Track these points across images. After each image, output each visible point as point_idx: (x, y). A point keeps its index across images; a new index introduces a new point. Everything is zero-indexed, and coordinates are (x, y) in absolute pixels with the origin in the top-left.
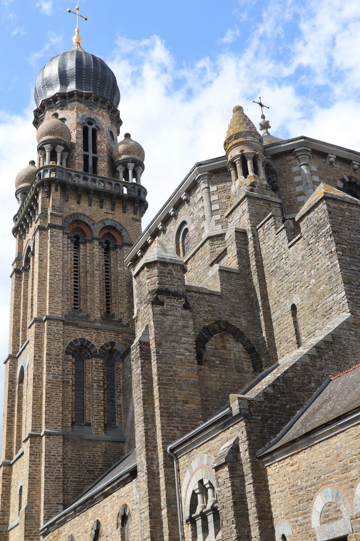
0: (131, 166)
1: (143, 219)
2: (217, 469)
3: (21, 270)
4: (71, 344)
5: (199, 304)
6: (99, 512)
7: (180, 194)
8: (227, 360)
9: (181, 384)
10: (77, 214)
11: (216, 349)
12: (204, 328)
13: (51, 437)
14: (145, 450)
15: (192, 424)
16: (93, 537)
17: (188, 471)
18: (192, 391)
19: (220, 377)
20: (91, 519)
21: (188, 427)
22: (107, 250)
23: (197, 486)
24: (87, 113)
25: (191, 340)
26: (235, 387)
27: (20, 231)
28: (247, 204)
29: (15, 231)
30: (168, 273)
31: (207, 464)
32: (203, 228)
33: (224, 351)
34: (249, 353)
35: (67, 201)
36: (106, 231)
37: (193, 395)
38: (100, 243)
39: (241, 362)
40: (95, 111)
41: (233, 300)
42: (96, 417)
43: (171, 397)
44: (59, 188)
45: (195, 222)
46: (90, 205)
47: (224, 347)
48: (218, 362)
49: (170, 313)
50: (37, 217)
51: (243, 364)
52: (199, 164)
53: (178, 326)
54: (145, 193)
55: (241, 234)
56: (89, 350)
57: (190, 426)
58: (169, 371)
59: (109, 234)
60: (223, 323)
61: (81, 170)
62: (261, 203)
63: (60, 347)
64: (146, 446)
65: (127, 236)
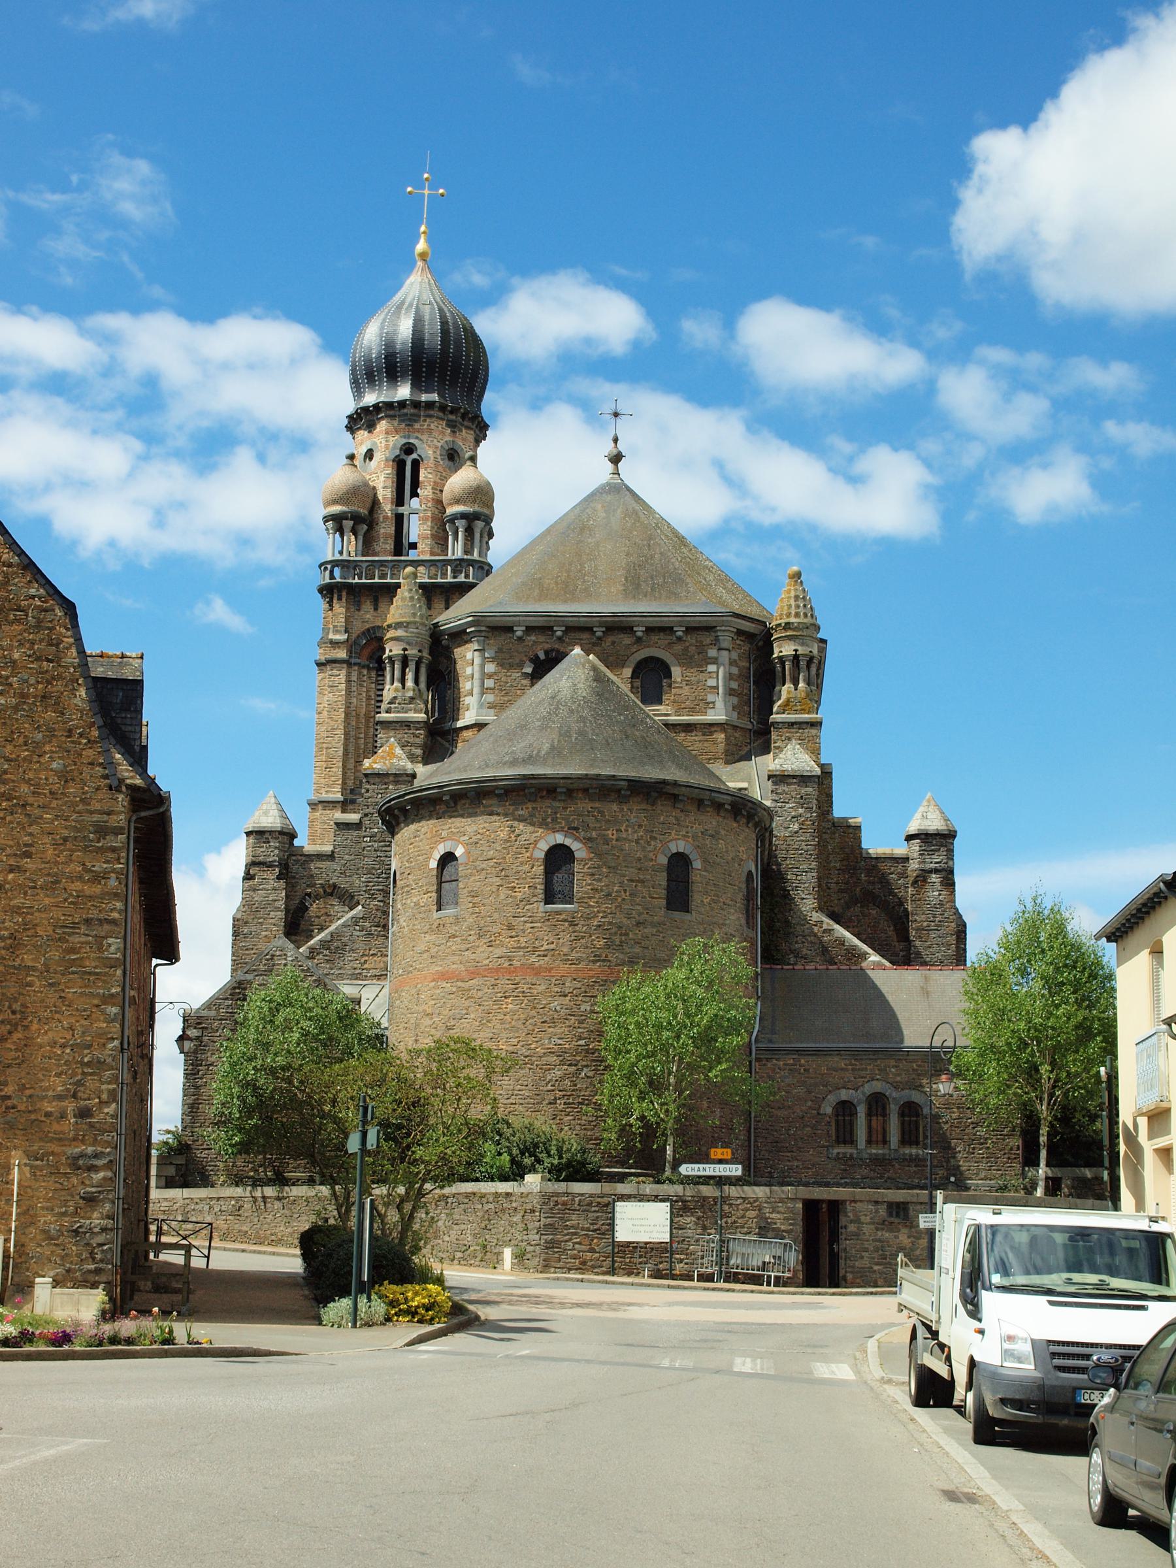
10: (373, 628)
35: (359, 610)
40: (417, 426)
44: (344, 594)
60: (330, 886)
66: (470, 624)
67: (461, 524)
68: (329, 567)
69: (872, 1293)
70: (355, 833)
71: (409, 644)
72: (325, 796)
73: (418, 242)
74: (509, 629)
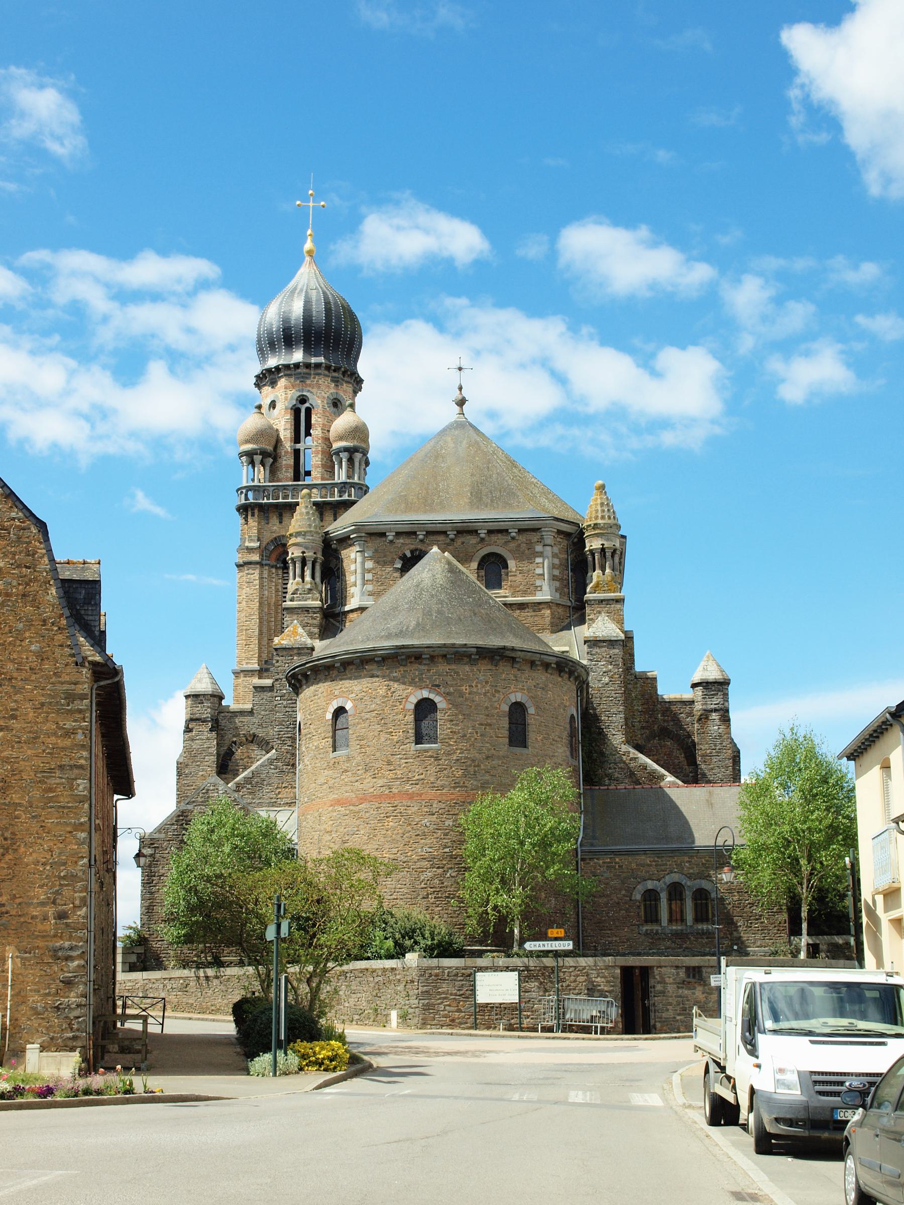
40: (308, 382)
44: (256, 511)
60: (250, 735)
66: (353, 532)
67: (344, 456)
68: (244, 491)
69: (676, 1038)
70: (269, 694)
71: (307, 548)
72: (246, 667)
73: (305, 242)
74: (383, 535)
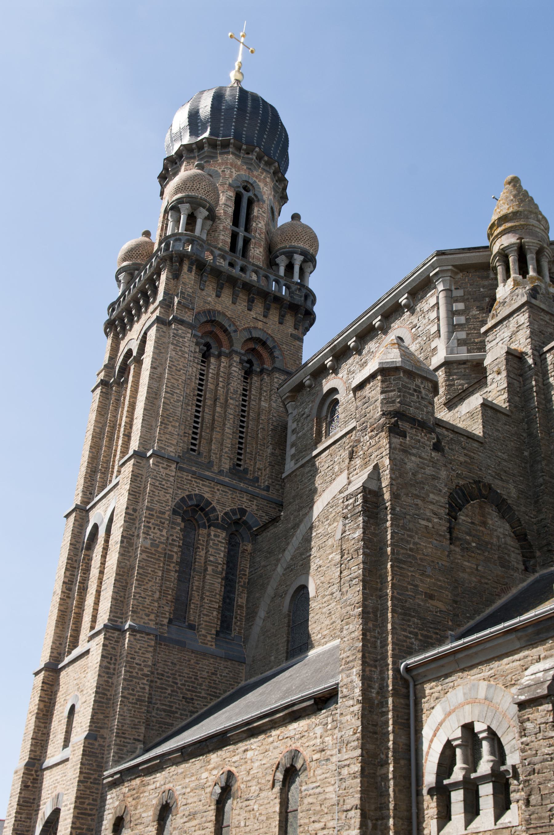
0: (298, 259)
1: (307, 338)
2: (522, 705)
3: (114, 381)
4: (183, 499)
5: (452, 450)
6: (235, 759)
7: (400, 295)
8: (487, 543)
9: (424, 566)
10: (214, 311)
11: (472, 523)
12: (457, 486)
13: (138, 635)
14: (360, 662)
15: (437, 633)
16: (216, 797)
17: (438, 708)
18: (440, 581)
19: (477, 570)
20: (214, 768)
21: (431, 638)
22: (248, 374)
23: (458, 733)
24: (244, 173)
25: (443, 500)
26: (497, 588)
27: (117, 325)
28: (527, 315)
29: (110, 325)
30: (415, 390)
31: (486, 699)
32: (435, 349)
33: (483, 529)
34: (519, 540)
36: (251, 345)
37: (441, 587)
38: (241, 362)
39: (506, 551)
41: (500, 454)
42: (206, 618)
43: (409, 583)
44: (194, 268)
45: (420, 339)
46: (234, 303)
47: (484, 524)
48: (474, 544)
49: (414, 451)
50: (157, 303)
51: (509, 555)
52: (440, 253)
53: (424, 473)
54: (314, 302)
55: (514, 358)
56: (206, 515)
57: (434, 636)
58: (408, 542)
59: (253, 350)
60: (484, 485)
61: (227, 249)
62: (547, 318)
63: (168, 500)
64: (363, 657)
65: (280, 358)
